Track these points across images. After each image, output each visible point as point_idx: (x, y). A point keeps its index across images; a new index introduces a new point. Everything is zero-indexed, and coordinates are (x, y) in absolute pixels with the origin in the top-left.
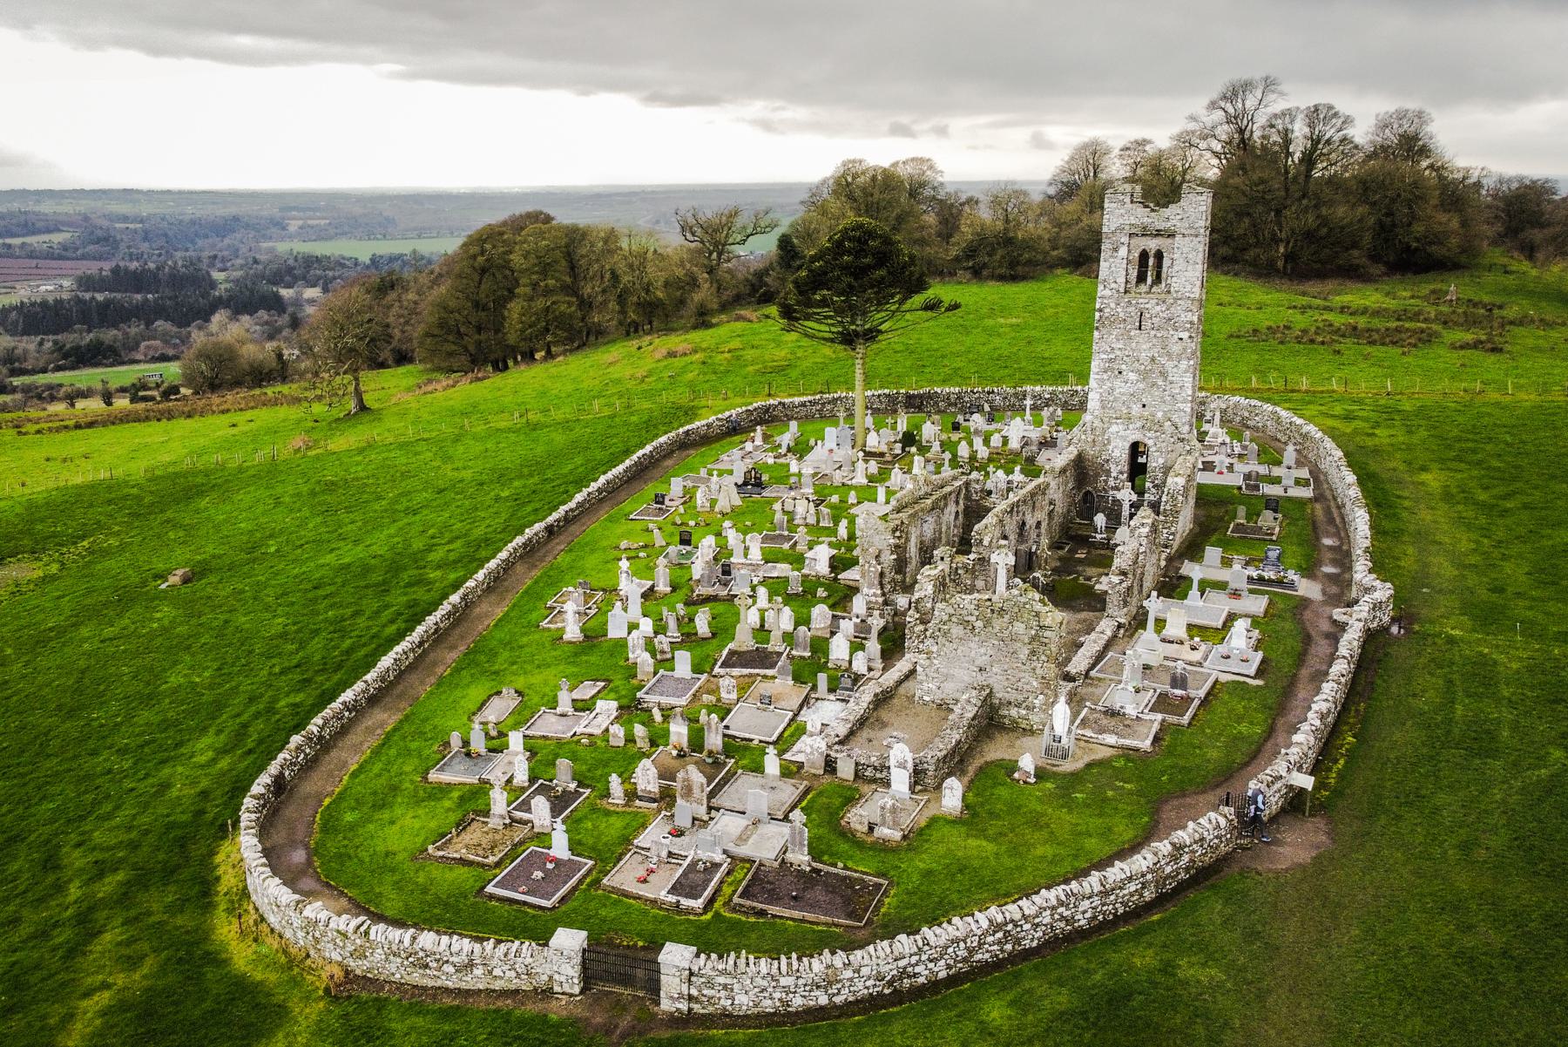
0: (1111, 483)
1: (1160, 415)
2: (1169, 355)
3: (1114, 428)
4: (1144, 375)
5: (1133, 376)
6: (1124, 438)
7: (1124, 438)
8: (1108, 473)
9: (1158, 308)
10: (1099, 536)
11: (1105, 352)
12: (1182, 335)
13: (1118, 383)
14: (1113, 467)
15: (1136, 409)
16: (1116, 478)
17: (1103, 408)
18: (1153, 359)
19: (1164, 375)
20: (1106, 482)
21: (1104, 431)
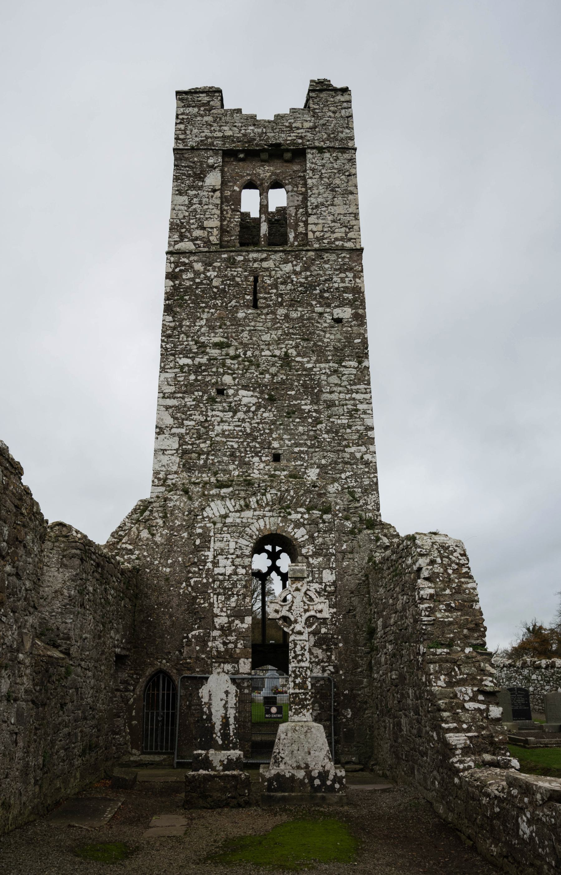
0: (217, 645)
1: (313, 474)
2: (320, 352)
3: (216, 509)
4: (271, 396)
5: (247, 397)
6: (239, 530)
7: (239, 530)
8: (205, 618)
9: (288, 268)
10: (218, 757)
11: (186, 353)
12: (338, 313)
13: (217, 414)
14: (217, 601)
15: (259, 468)
16: (226, 631)
17: (188, 467)
18: (286, 360)
19: (312, 390)
20: (203, 641)
21: (193, 517)
